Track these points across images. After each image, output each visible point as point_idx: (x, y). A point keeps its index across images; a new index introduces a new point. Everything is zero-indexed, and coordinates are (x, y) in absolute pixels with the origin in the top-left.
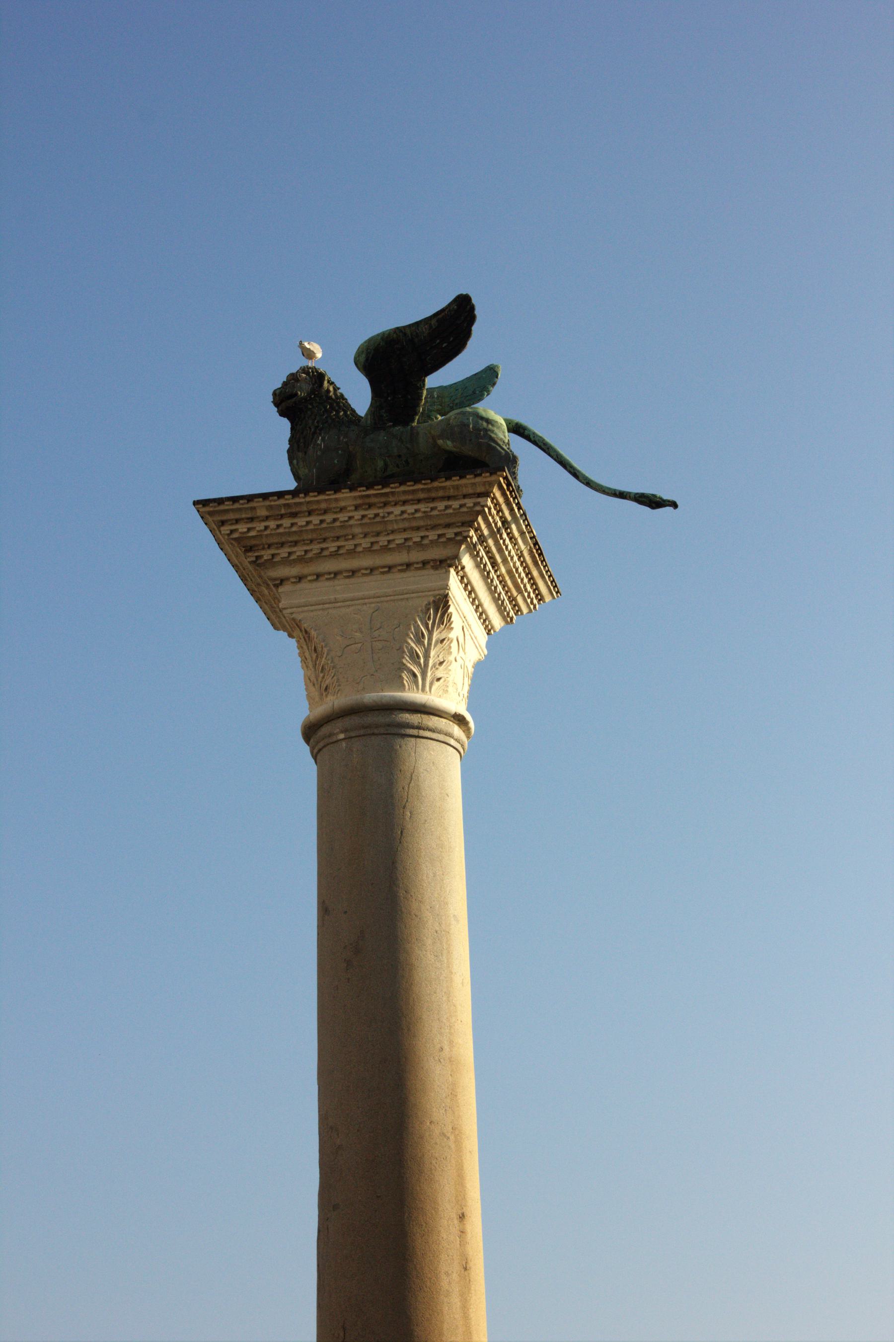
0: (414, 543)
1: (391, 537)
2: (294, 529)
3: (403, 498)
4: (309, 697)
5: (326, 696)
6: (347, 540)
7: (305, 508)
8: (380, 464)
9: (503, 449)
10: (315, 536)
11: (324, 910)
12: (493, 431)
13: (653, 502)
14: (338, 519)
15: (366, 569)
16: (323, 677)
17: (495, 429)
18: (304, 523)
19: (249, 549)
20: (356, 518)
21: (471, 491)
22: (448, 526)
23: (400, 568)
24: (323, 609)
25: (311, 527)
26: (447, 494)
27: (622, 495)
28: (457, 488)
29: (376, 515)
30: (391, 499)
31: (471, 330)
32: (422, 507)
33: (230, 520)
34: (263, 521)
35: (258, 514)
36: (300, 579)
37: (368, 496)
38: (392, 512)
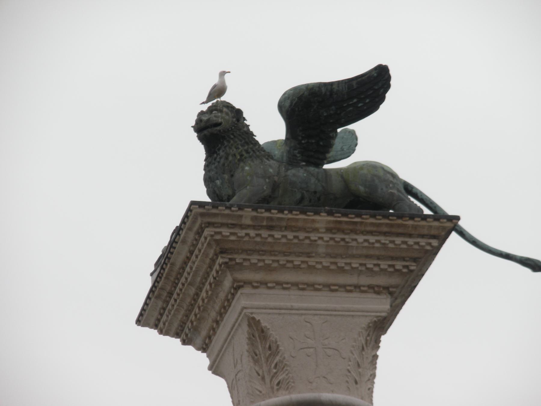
0: (367, 269)
1: (348, 261)
3: (369, 228)
5: (278, 390)
6: (309, 257)
7: (284, 224)
15: (319, 285)
16: (276, 373)
20: (325, 239)
21: (425, 232)
23: (348, 288)
24: (280, 314)
28: (415, 227)
29: (343, 240)
30: (358, 227)
32: (383, 239)
33: (216, 223)
37: (340, 222)
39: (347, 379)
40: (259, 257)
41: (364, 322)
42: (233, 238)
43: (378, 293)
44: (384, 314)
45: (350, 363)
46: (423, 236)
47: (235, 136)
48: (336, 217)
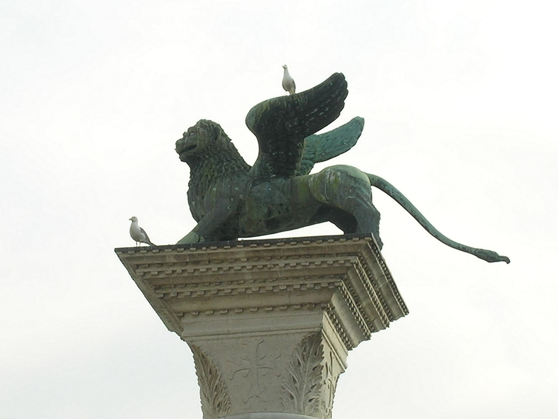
1: (275, 284)
2: (196, 274)
6: (239, 284)
7: (206, 258)
8: (266, 210)
10: (213, 280)
12: (360, 188)
13: (490, 257)
14: (233, 268)
15: (254, 308)
16: (217, 395)
17: (361, 186)
18: (205, 270)
19: (158, 288)
20: (248, 267)
21: (342, 250)
22: (322, 277)
25: (210, 273)
26: (323, 252)
29: (265, 266)
30: (277, 253)
32: (304, 262)
34: (171, 266)
35: (167, 261)
36: (199, 312)
38: (278, 265)
39: (281, 396)
41: (299, 338)
42: (162, 276)
43: (311, 309)
45: (284, 380)
46: (342, 254)
48: (252, 247)
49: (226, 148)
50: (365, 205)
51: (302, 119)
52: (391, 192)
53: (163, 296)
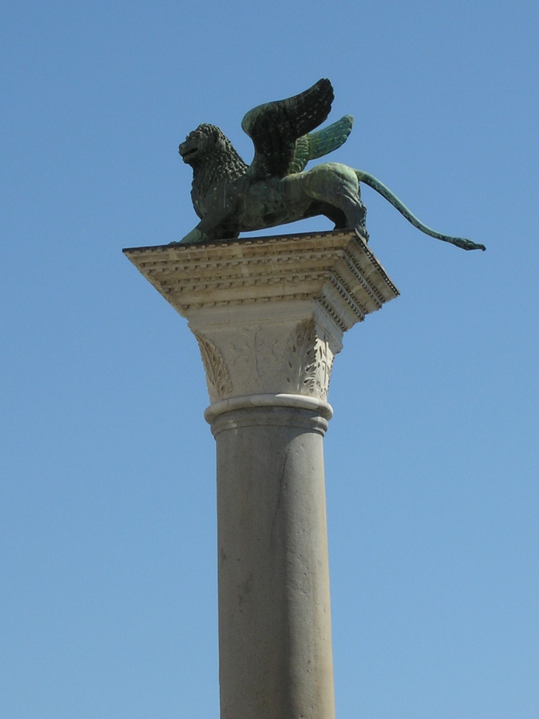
3: (279, 249)
4: (212, 394)
5: (223, 394)
7: (205, 255)
8: (262, 207)
9: (355, 201)
11: (223, 556)
12: (347, 185)
13: (468, 246)
15: (252, 299)
18: (205, 266)
20: (244, 263)
22: (312, 270)
27: (444, 238)
29: (259, 262)
31: (330, 107)
35: (171, 259)
38: (271, 259)
40: (194, 284)
44: (309, 316)
46: (330, 249)
47: (210, 159)
49: (225, 150)
50: (351, 200)
51: (291, 124)
52: (376, 187)
53: (168, 290)
